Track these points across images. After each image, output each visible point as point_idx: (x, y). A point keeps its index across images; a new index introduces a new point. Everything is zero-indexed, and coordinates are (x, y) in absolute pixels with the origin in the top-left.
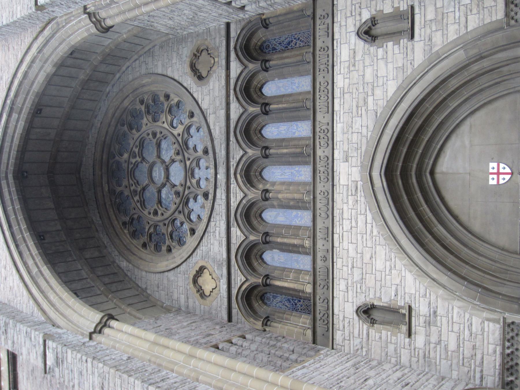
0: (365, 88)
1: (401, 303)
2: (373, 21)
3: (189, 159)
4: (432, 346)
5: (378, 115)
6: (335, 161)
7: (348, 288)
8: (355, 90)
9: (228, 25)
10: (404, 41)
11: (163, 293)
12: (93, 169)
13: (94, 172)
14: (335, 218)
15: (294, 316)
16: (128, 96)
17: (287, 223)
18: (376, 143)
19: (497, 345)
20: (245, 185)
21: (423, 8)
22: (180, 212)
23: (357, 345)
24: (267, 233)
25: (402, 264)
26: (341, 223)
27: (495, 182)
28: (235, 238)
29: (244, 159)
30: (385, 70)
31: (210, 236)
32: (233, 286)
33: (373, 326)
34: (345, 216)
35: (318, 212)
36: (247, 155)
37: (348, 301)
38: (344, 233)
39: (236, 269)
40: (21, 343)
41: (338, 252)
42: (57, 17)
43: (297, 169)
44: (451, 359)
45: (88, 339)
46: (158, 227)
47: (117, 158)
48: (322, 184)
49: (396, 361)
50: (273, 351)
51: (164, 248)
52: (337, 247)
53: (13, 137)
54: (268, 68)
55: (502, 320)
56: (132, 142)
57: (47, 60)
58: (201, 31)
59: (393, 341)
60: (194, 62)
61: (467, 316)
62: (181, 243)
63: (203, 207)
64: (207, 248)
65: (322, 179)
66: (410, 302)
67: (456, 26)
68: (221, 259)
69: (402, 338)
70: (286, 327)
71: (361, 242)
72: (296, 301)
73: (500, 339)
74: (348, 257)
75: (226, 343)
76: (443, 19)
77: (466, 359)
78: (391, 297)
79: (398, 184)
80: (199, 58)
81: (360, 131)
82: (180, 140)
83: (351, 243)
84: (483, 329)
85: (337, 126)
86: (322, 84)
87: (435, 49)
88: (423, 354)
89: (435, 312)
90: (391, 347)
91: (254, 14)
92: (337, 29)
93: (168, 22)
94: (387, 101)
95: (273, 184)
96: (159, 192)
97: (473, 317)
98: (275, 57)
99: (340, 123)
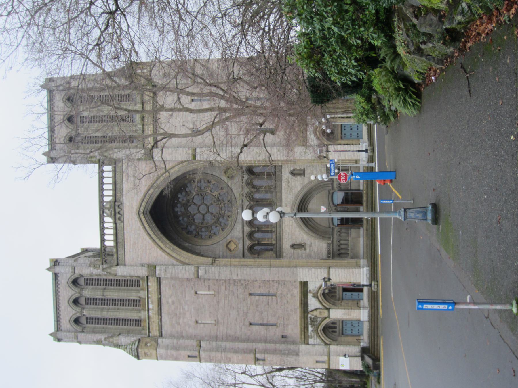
2: (294, 170)
10: (302, 177)
90: (300, 254)
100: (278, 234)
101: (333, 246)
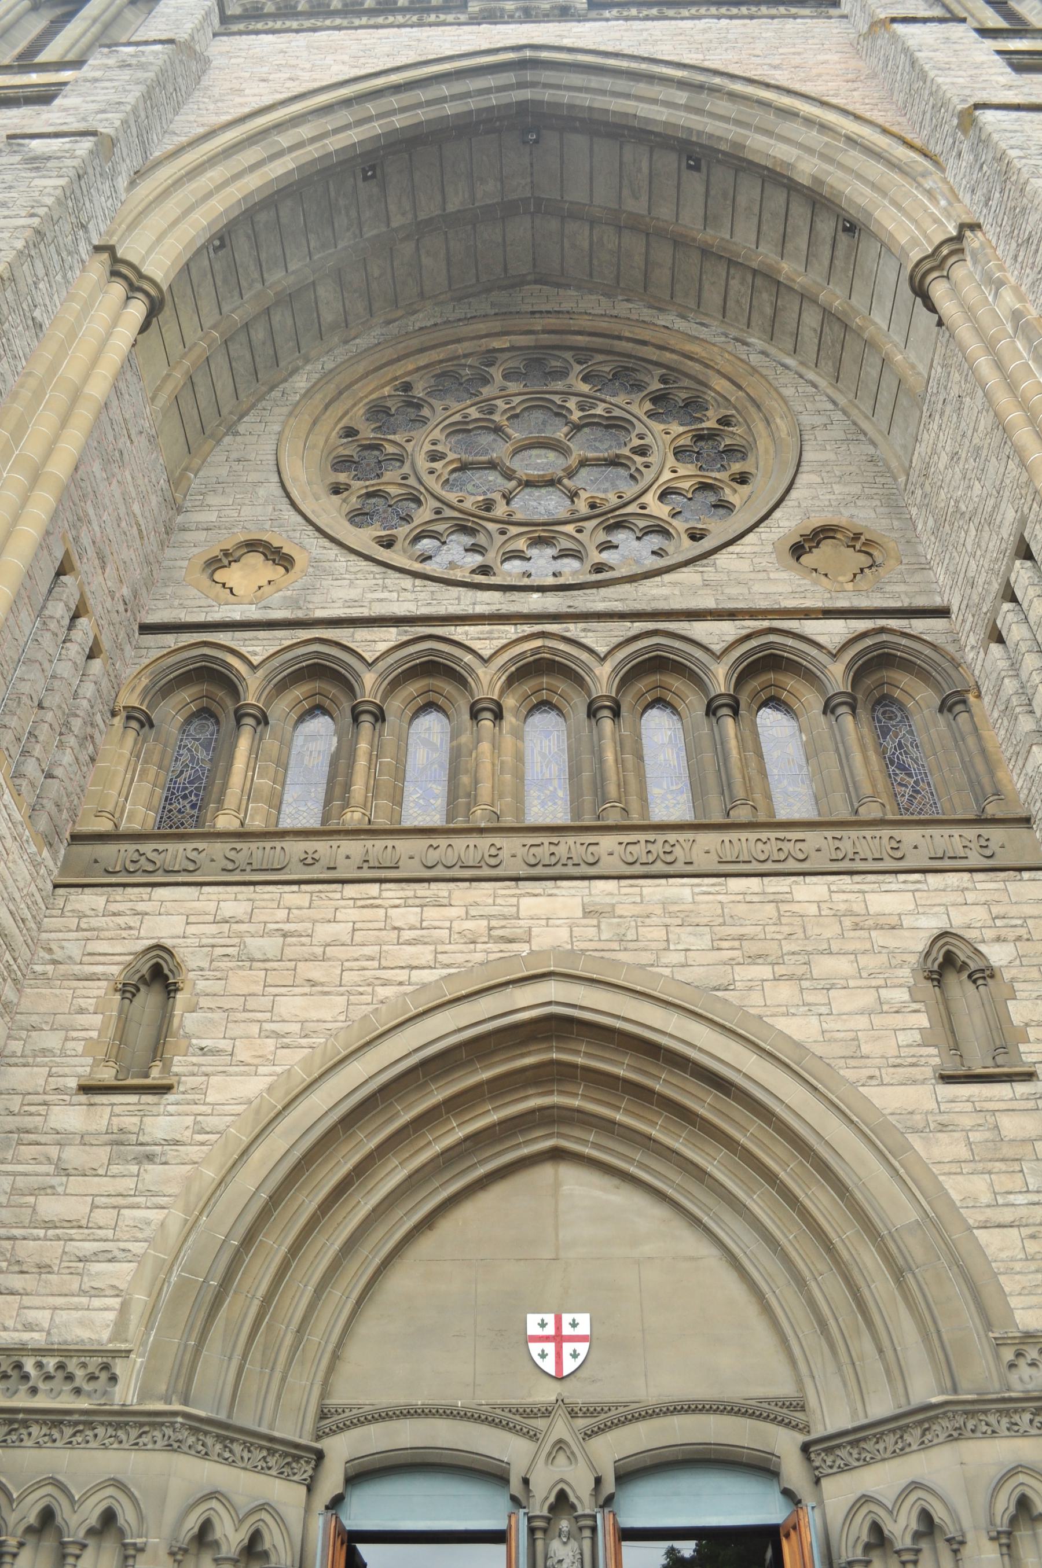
0: (795, 957)
1: (179, 1064)
3: (579, 531)
4: (53, 1151)
5: (719, 994)
6: (586, 883)
7: (227, 922)
8: (786, 930)
9: (943, 612)
10: (933, 1057)
11: (223, 471)
12: (548, 312)
13: (541, 312)
14: (426, 885)
15: (153, 791)
16: (740, 387)
17: (409, 775)
18: (638, 988)
19: (49, 1333)
20: (513, 660)
21: (1031, 1104)
22: (438, 512)
23: (63, 948)
24: (384, 720)
25: (292, 1066)
26: (410, 902)
27: (533, 1328)
28: (369, 638)
29: (584, 656)
30: (847, 1008)
31: (375, 578)
32: (239, 635)
33: (116, 990)
34: (430, 913)
35: (442, 842)
36: (596, 664)
37: (188, 923)
38: (382, 911)
39: (283, 642)
40: (93, 95)
41: (331, 895)
42: (943, 170)
43: (560, 793)
44: (12, 1203)
45: (96, 242)
46: (398, 464)
47: (578, 368)
48: (521, 852)
49: (13, 1055)
50: (49, 716)
51: (342, 477)
52: (341, 892)
53: (628, 96)
54: (833, 712)
55: (123, 1346)
56: (620, 399)
57: (830, 160)
58: (920, 549)
59: (70, 1045)
60: (839, 536)
61: (138, 1248)
62: (358, 517)
63: (452, 565)
64: (343, 571)
65: (533, 850)
66: (182, 1089)
67: (986, 1198)
68: (311, 606)
69: (80, 1070)
70: (121, 769)
71: (356, 955)
72: (193, 798)
73: (65, 1343)
74: (314, 922)
75: (77, 596)
76: (1002, 1160)
77: (10, 1247)
78: (198, 1038)
79: (523, 1055)
80: (848, 546)
81: (672, 947)
82: (629, 509)
83: (354, 930)
84: (97, 1292)
85: (683, 885)
86: (799, 845)
87: (916, 1141)
88: (30, 1126)
89: (150, 1158)
91: (977, 673)
92: (955, 880)
93: (944, 456)
94: (760, 1017)
95: (518, 735)
96: (492, 465)
97: (135, 1265)
98: (865, 731)
99: (693, 894)
100: (297, 848)
101: (55, 1419)
